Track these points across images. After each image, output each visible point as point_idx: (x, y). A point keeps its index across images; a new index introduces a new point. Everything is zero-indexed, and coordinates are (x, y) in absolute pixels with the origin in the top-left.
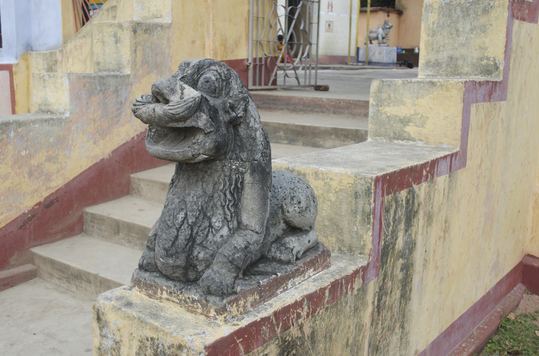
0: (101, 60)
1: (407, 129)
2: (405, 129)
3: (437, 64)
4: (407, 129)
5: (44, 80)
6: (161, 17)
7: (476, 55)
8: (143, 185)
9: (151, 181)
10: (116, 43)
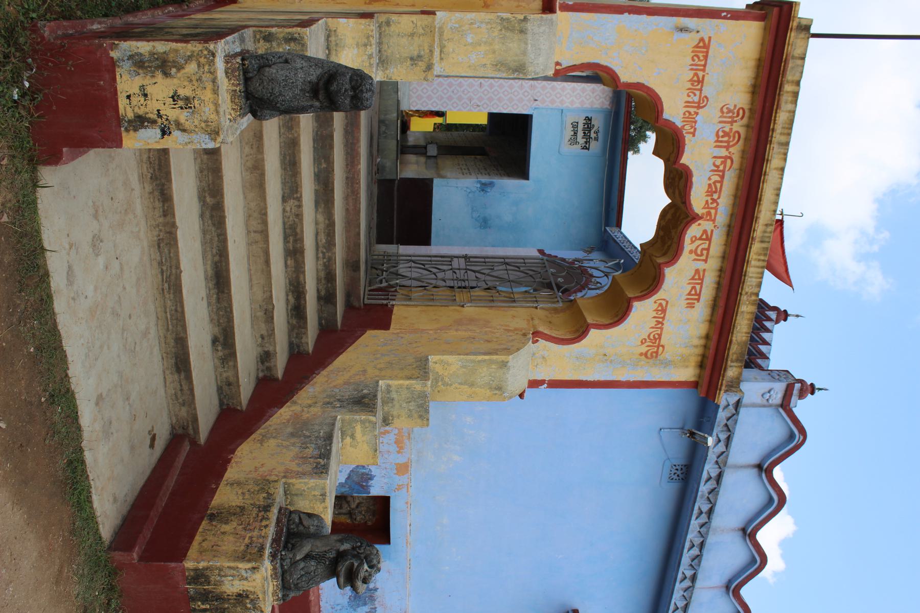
0: (393, 28)
1: (348, 438)
3: (389, 391)
4: (348, 438)
5: (365, 45)
6: (441, 59)
7: (395, 413)
10: (412, 59)
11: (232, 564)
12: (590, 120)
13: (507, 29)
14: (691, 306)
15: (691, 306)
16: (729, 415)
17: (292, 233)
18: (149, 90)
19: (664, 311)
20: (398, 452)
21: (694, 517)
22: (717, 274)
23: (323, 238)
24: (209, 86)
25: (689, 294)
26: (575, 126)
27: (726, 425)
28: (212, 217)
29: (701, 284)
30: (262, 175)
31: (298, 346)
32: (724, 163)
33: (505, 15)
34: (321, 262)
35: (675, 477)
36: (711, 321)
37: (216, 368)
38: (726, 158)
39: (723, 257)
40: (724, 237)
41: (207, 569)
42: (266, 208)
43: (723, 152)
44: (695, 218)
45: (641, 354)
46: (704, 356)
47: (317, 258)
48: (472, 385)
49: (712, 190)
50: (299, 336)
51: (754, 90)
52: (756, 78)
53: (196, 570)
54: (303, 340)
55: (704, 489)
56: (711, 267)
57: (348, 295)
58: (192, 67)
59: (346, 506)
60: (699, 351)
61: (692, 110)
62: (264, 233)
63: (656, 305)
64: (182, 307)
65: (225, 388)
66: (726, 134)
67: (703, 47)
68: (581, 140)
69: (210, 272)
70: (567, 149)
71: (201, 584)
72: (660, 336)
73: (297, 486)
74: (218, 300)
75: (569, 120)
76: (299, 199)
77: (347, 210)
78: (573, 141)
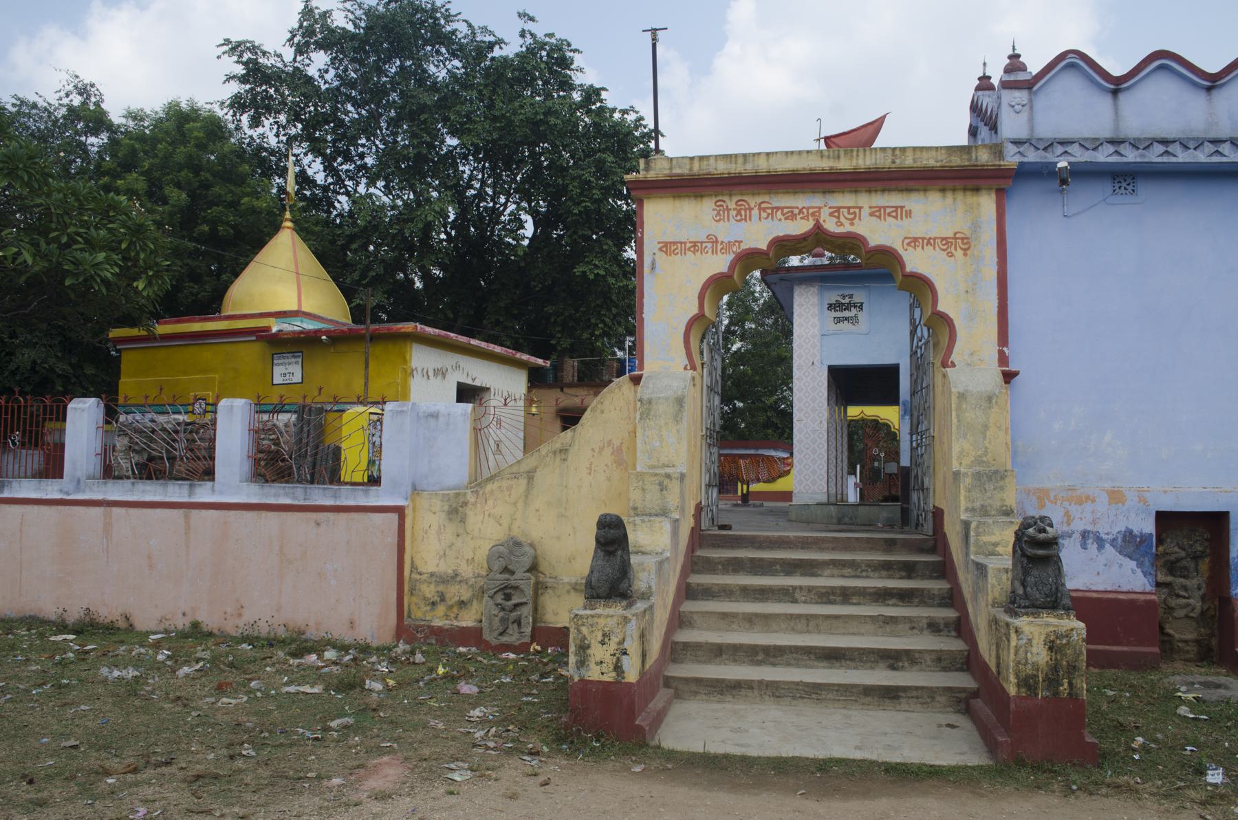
0: (638, 505)
2: (1090, 541)
3: (973, 510)
8: (695, 617)
9: (707, 613)
11: (1012, 651)
12: (830, 305)
13: (648, 415)
14: (909, 214)
15: (909, 214)
16: (1032, 149)
17: (826, 596)
18: (598, 660)
19: (915, 240)
20: (1093, 501)
21: (1173, 159)
22: (873, 194)
23: (847, 571)
24: (596, 620)
25: (896, 218)
26: (838, 320)
27: (1045, 149)
28: (774, 656)
29: (885, 208)
30: (757, 615)
31: (944, 598)
32: (764, 210)
33: (638, 417)
34: (871, 574)
35: (1130, 188)
36: (925, 190)
37: (922, 670)
38: (760, 209)
39: (856, 192)
40: (835, 195)
41: (1017, 676)
42: (786, 615)
43: (755, 212)
44: (818, 226)
45: (965, 255)
46: (965, 190)
47: (867, 577)
48: (986, 427)
49: (791, 216)
50: (932, 597)
51: (699, 196)
52: (689, 197)
53: (1018, 686)
54: (936, 593)
55: (1131, 156)
56: (865, 201)
57: (922, 551)
58: (584, 630)
59: (1184, 563)
60: (960, 196)
61: (719, 247)
62: (809, 618)
63: (910, 249)
64: (834, 685)
65: (944, 664)
66: (739, 213)
67: (667, 247)
68: (854, 311)
69: (825, 664)
70: (863, 326)
71: (1036, 683)
72: (943, 239)
73: (997, 595)
74: (851, 660)
75: (832, 327)
76: (794, 588)
77: (833, 549)
78: (854, 320)
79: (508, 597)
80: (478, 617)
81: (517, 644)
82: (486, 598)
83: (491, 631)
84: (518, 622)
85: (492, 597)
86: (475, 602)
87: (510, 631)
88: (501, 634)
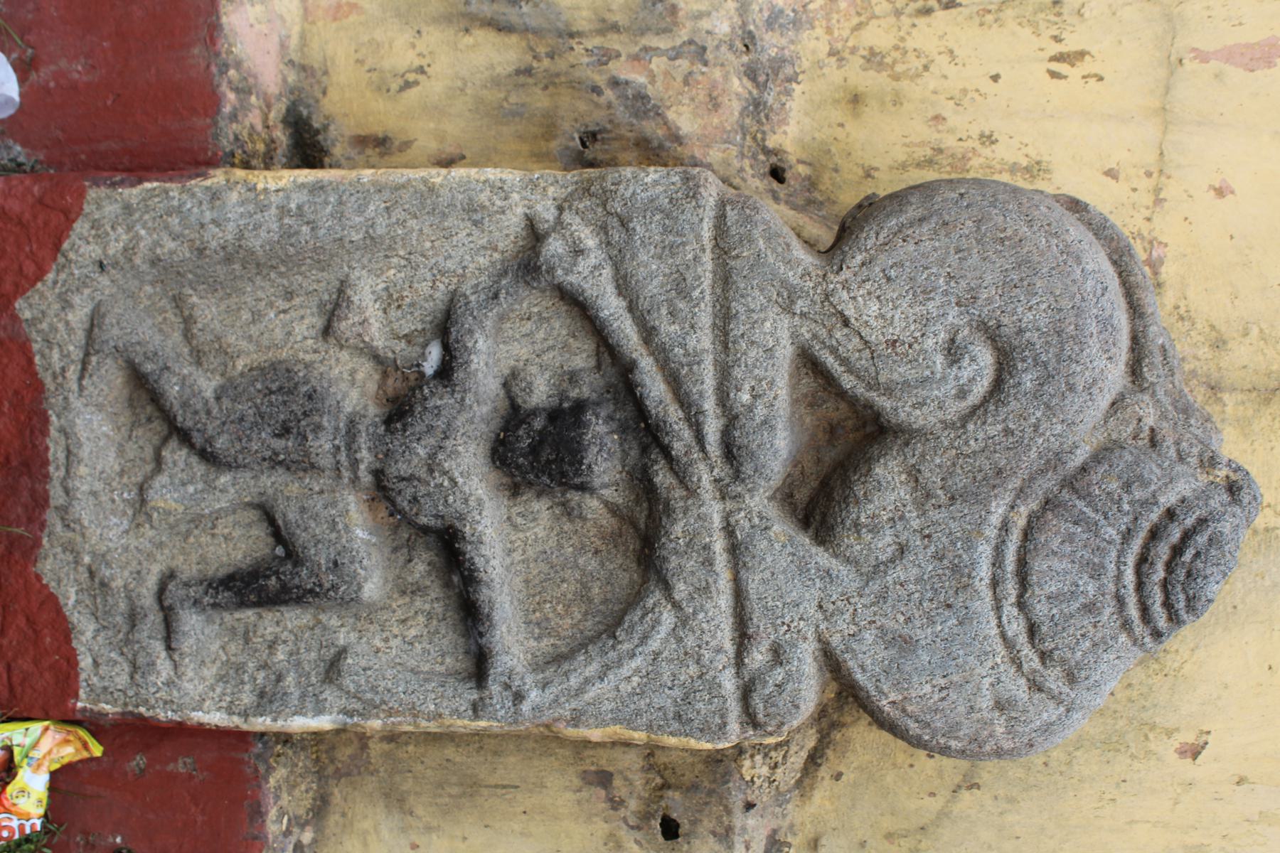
79: (537, 450)
80: (346, 106)
81: (56, 570)
82: (520, 191)
83: (172, 280)
84: (272, 579)
85: (528, 262)
86: (493, 54)
87: (179, 484)
88: (143, 388)
